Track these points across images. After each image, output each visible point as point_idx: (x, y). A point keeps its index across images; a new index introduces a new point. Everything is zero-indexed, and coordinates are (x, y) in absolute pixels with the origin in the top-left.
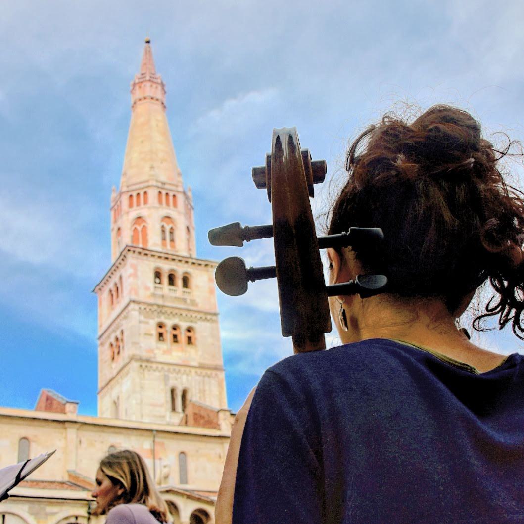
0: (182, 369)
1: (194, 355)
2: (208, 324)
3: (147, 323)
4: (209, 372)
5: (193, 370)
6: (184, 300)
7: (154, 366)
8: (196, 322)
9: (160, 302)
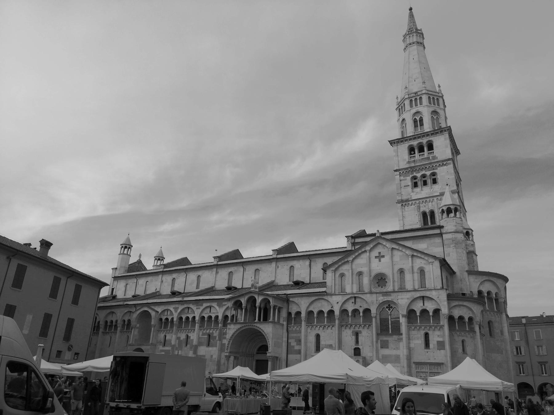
0: (428, 200)
1: (436, 189)
3: (406, 179)
5: (435, 199)
7: (410, 203)
9: (413, 165)
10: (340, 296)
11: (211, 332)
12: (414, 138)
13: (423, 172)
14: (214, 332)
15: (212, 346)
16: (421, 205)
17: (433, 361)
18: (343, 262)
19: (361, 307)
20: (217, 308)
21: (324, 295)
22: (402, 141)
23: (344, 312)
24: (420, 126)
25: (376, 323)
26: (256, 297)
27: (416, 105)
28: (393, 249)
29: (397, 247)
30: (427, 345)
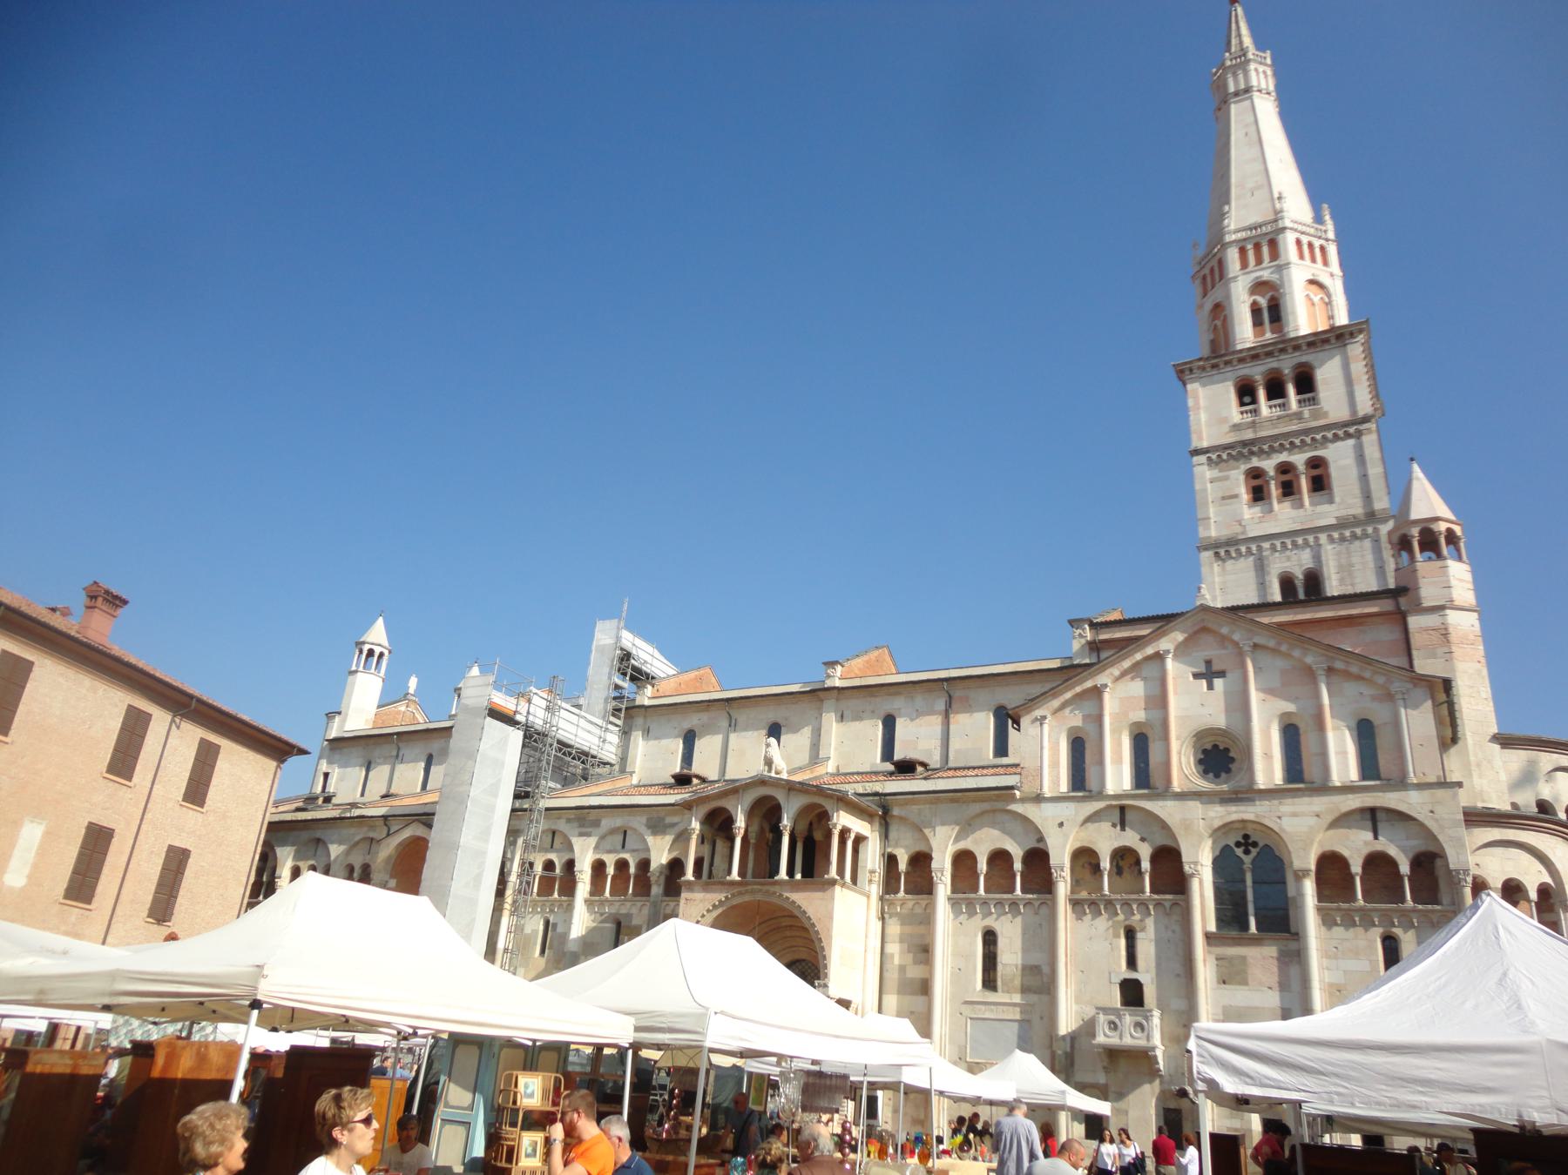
2: (1351, 442)
3: (1227, 478)
4: (1358, 531)
5: (1323, 538)
10: (1072, 806)
11: (623, 911)
12: (1254, 355)
13: (1283, 457)
14: (634, 911)
18: (1078, 689)
21: (1013, 799)
22: (1214, 366)
23: (1085, 858)
24: (1272, 321)
25: (1202, 896)
26: (780, 797)
27: (1259, 261)
28: (1256, 646)
29: (1272, 643)
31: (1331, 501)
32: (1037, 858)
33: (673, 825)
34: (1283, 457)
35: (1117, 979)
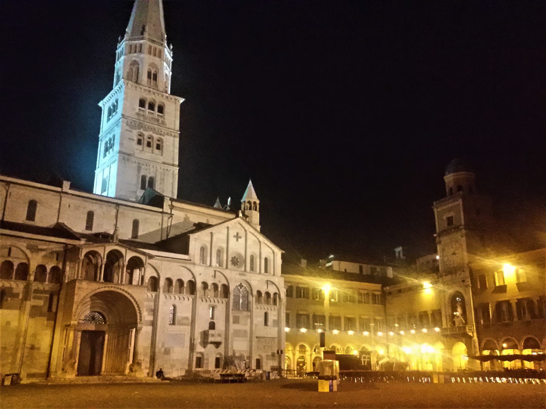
3: (132, 132)
6: (158, 120)
8: (164, 136)
13: (151, 133)
15: (8, 308)
16: (143, 167)
17: (270, 336)
19: (220, 281)
20: (28, 252)
26: (123, 250)
30: (266, 323)
31: (162, 155)
32: (192, 285)
33: (42, 250)
34: (151, 133)
35: (209, 322)
